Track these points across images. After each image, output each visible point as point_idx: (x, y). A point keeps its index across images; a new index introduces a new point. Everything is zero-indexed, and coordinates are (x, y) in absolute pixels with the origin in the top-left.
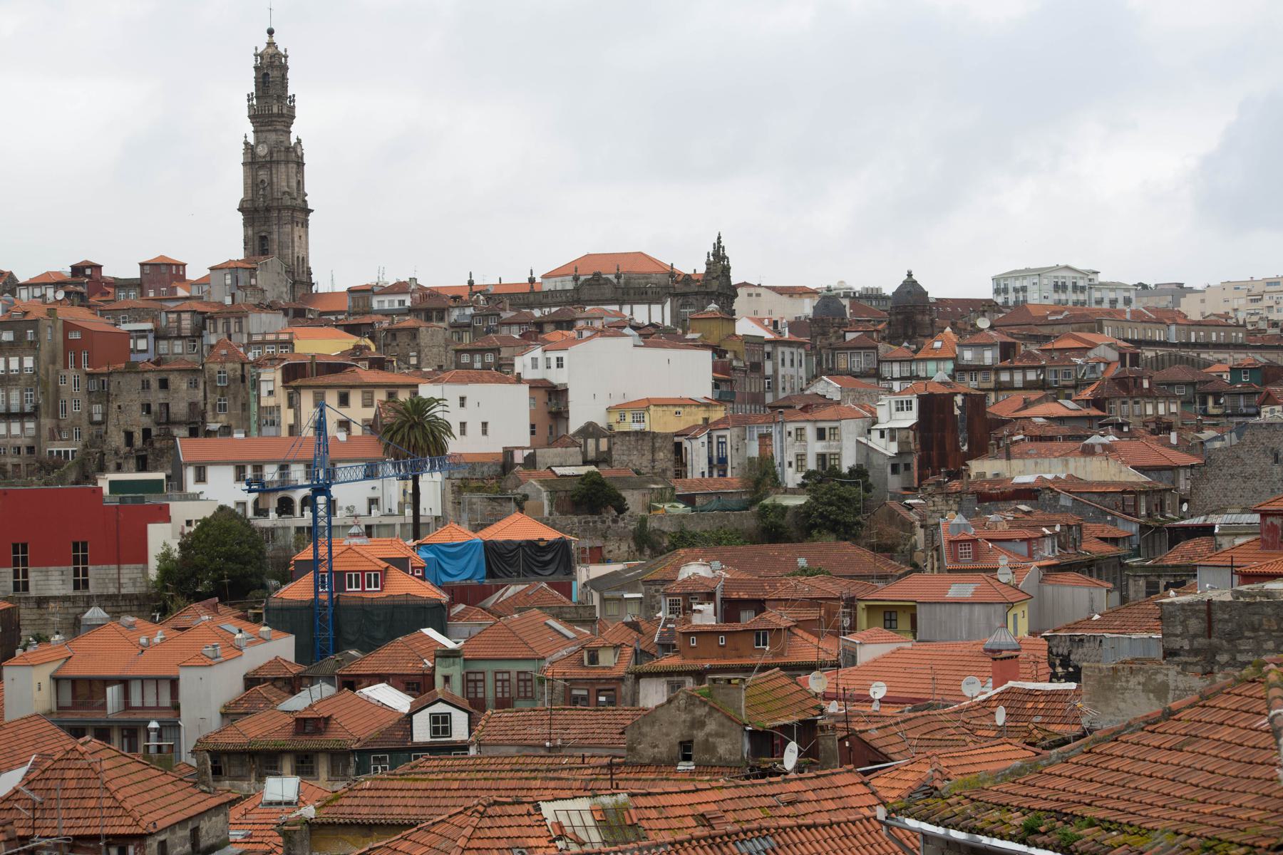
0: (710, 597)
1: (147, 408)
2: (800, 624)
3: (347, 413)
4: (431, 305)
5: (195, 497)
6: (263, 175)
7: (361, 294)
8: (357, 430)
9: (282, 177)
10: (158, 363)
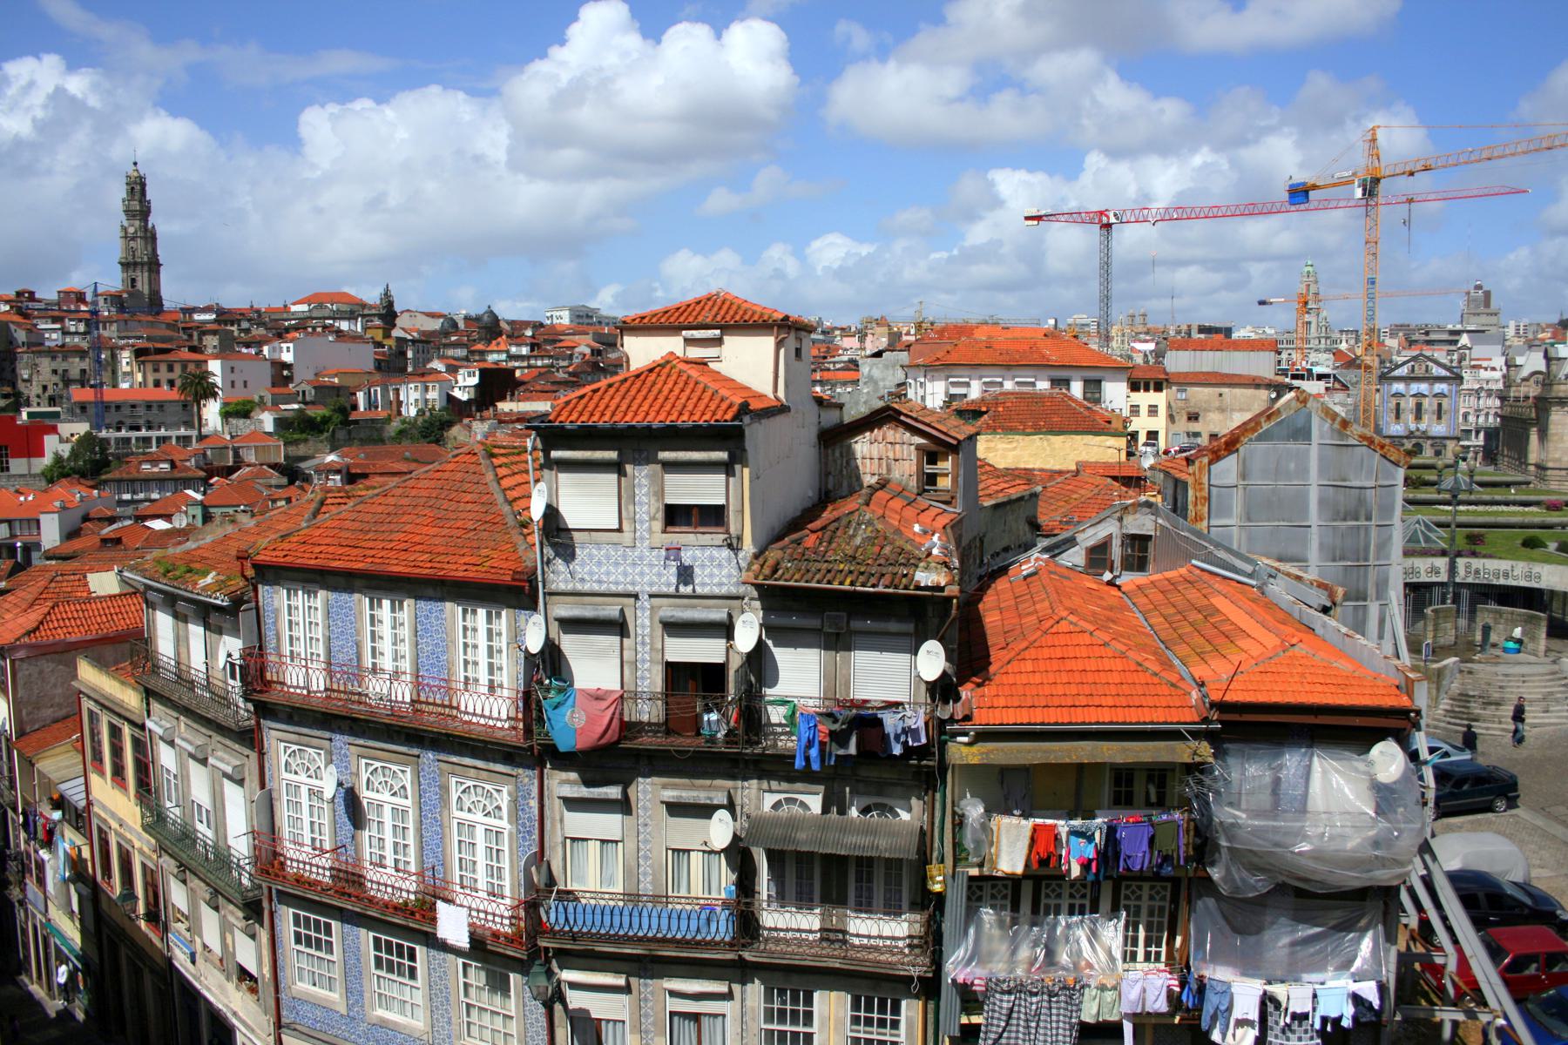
0: (338, 472)
1: (55, 372)
3: (171, 376)
4: (225, 317)
6: (132, 244)
10: (63, 346)
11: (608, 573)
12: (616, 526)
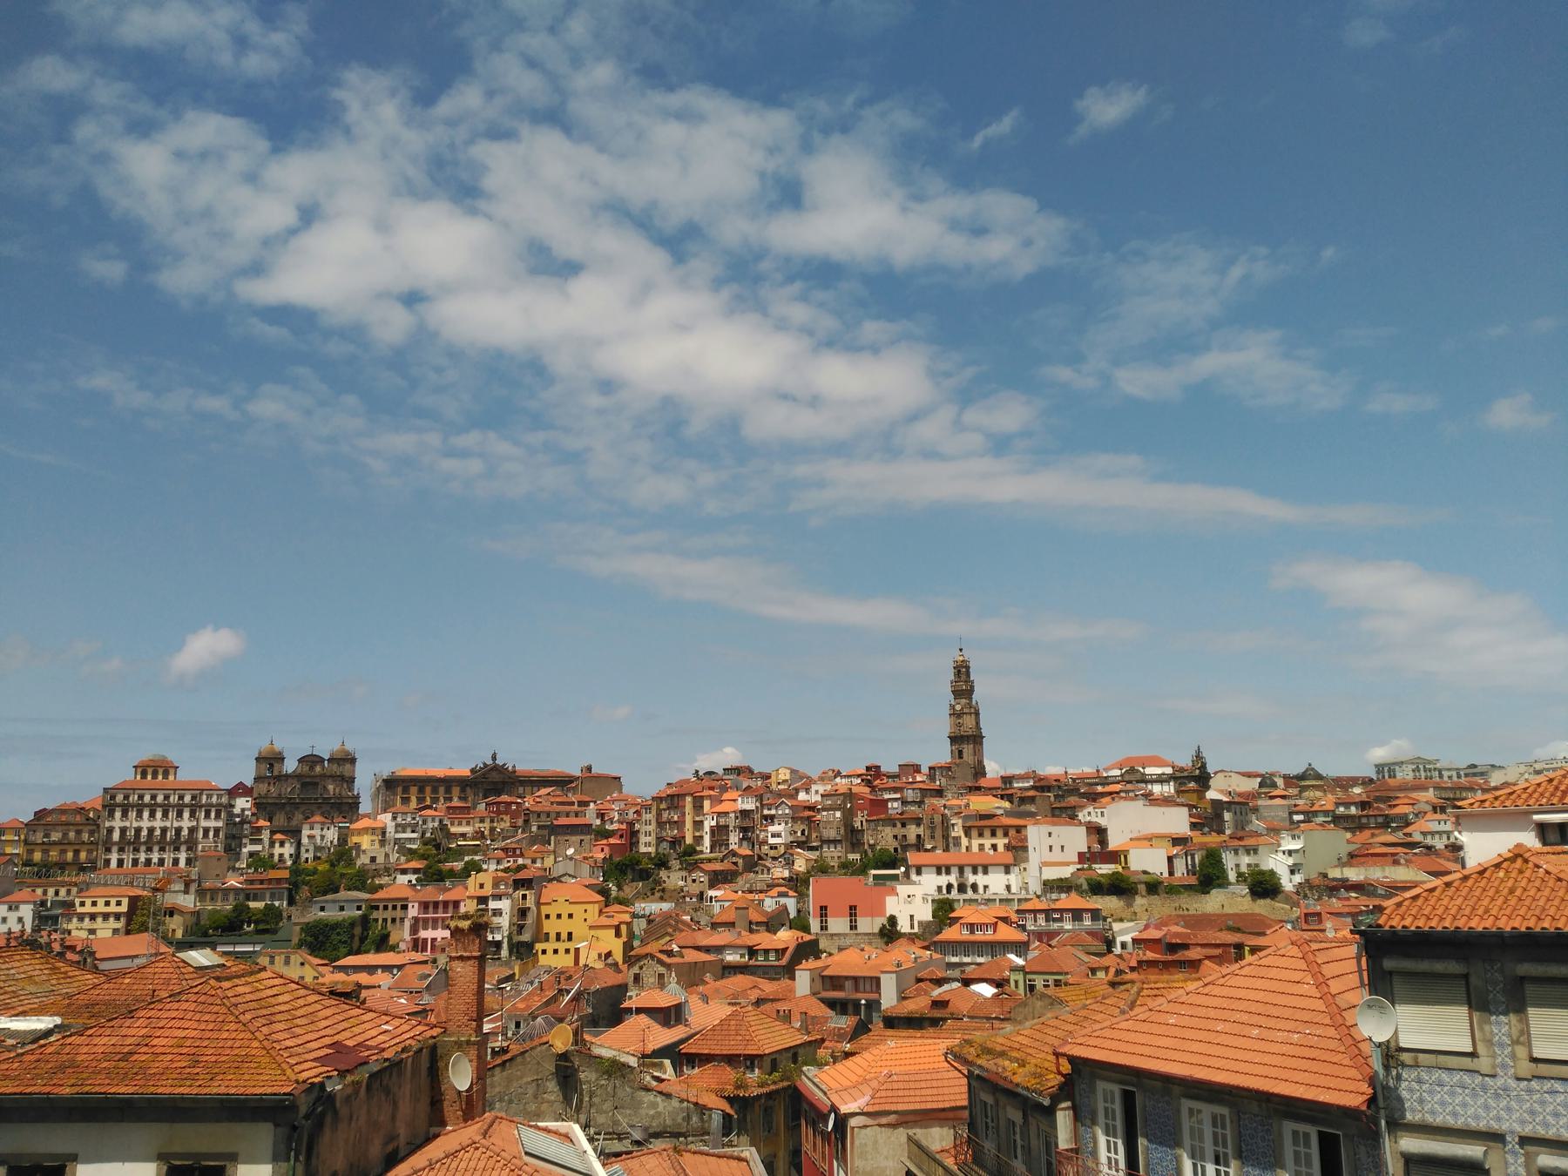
1: (895, 837)
2: (1208, 958)
4: (1043, 785)
5: (914, 883)
7: (1007, 780)
8: (1001, 848)
9: (968, 721)
11: (1464, 1105)
12: (1470, 1049)
